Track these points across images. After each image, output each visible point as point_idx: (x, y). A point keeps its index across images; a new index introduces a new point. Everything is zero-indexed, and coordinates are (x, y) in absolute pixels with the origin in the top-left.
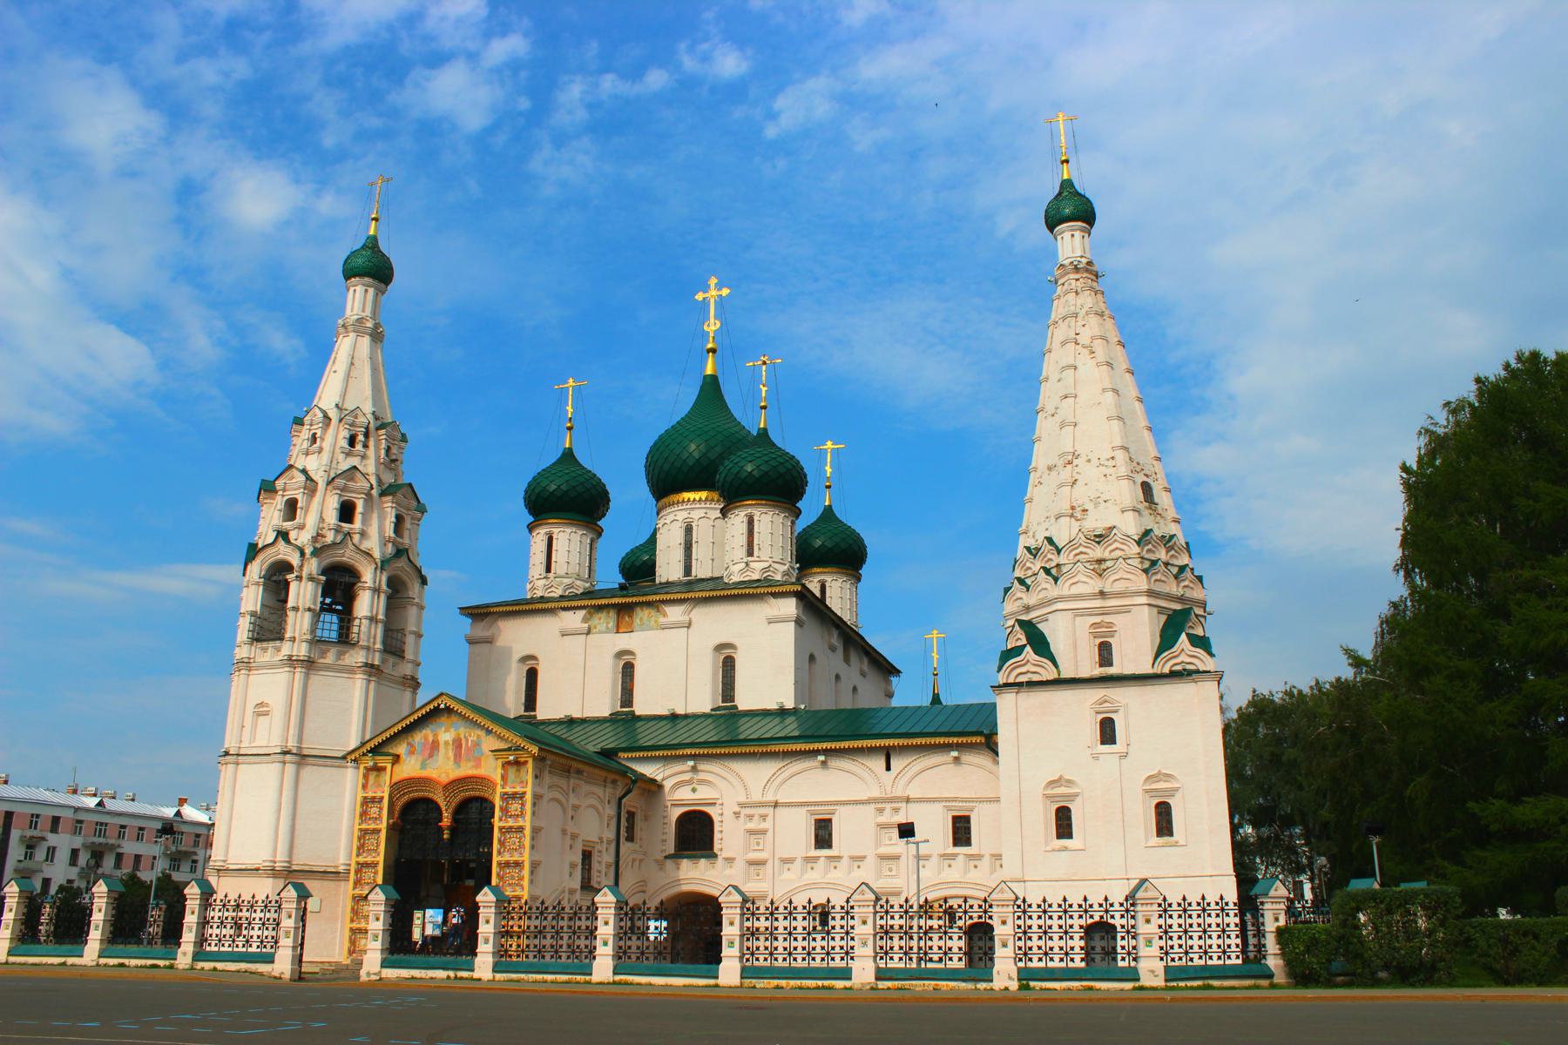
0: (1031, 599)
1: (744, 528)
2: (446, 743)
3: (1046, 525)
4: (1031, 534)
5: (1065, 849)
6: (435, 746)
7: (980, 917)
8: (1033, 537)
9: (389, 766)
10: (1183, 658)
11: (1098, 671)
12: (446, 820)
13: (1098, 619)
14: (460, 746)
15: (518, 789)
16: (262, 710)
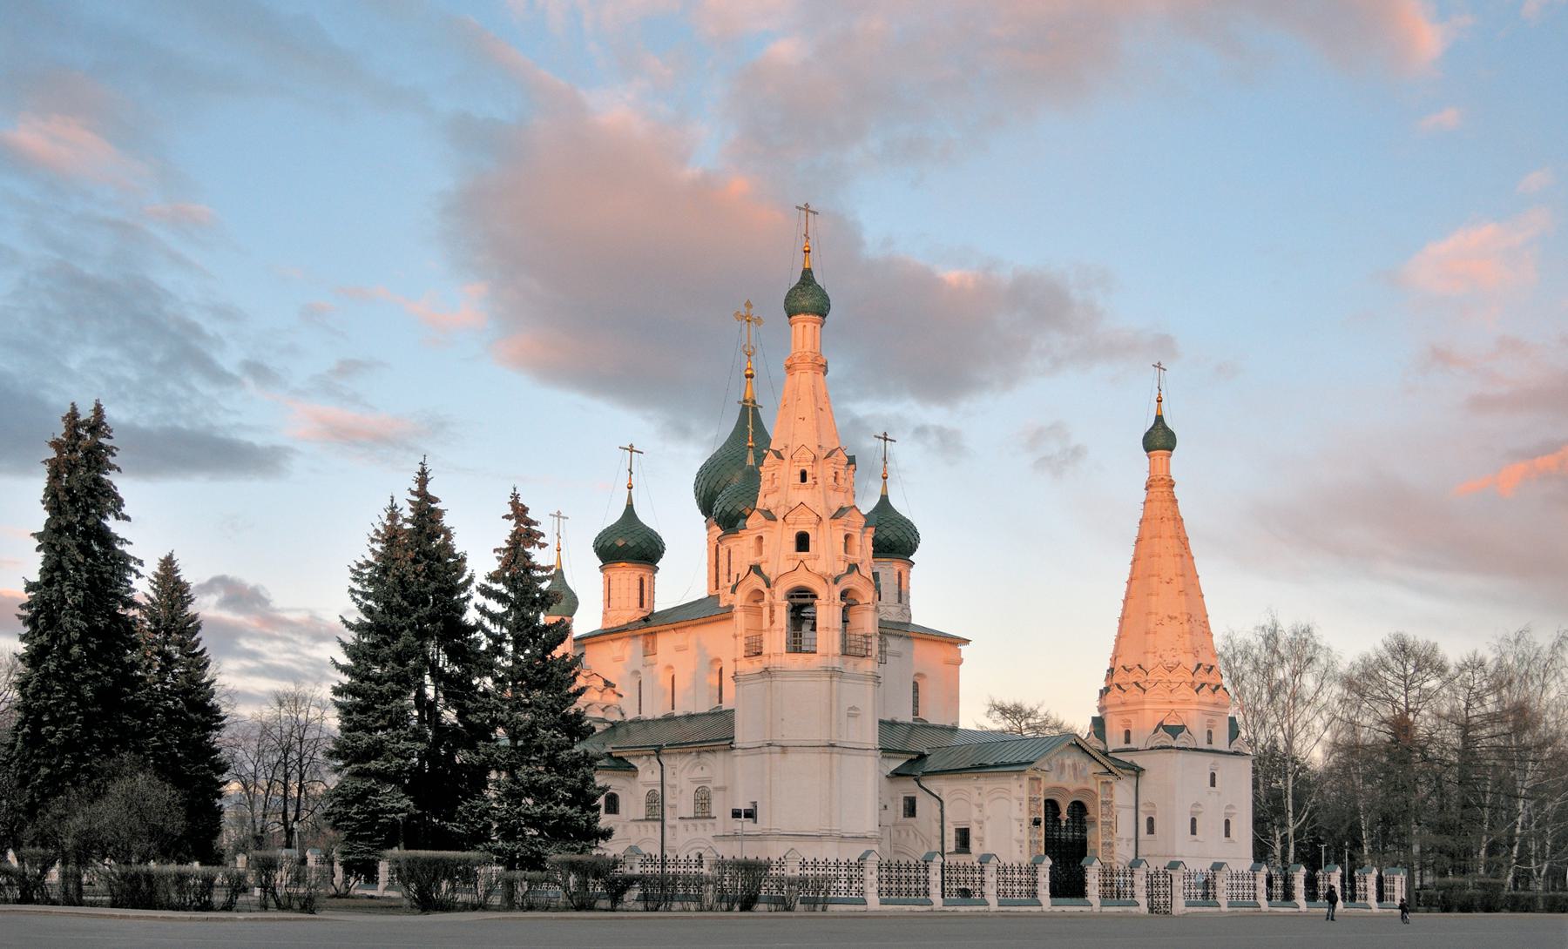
0: (1173, 698)
1: (897, 577)
2: (1069, 766)
3: (1173, 653)
4: (1158, 654)
5: (1196, 841)
6: (1063, 766)
7: (658, 867)
8: (1161, 657)
9: (1043, 778)
10: (1237, 745)
11: (1206, 746)
12: (1064, 815)
13: (1210, 717)
14: (1075, 769)
15: (1108, 799)
16: (853, 713)
